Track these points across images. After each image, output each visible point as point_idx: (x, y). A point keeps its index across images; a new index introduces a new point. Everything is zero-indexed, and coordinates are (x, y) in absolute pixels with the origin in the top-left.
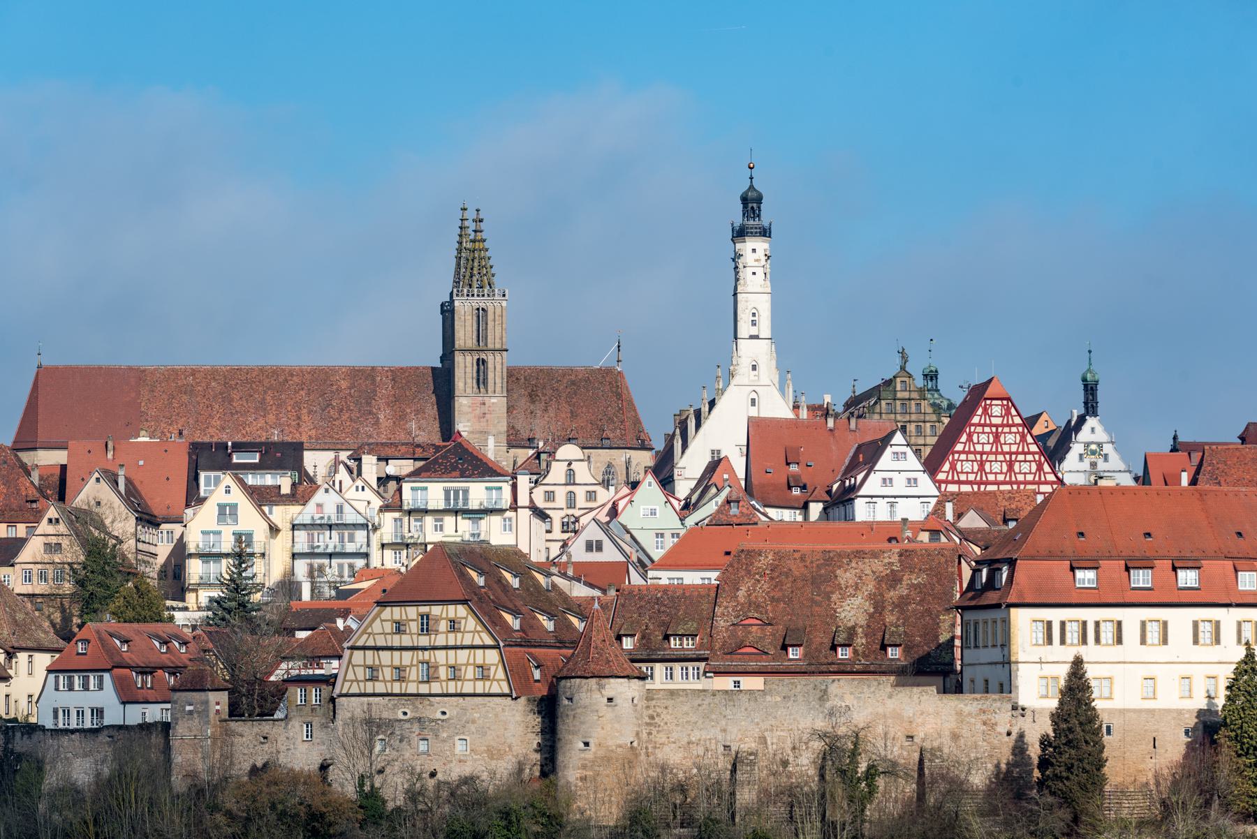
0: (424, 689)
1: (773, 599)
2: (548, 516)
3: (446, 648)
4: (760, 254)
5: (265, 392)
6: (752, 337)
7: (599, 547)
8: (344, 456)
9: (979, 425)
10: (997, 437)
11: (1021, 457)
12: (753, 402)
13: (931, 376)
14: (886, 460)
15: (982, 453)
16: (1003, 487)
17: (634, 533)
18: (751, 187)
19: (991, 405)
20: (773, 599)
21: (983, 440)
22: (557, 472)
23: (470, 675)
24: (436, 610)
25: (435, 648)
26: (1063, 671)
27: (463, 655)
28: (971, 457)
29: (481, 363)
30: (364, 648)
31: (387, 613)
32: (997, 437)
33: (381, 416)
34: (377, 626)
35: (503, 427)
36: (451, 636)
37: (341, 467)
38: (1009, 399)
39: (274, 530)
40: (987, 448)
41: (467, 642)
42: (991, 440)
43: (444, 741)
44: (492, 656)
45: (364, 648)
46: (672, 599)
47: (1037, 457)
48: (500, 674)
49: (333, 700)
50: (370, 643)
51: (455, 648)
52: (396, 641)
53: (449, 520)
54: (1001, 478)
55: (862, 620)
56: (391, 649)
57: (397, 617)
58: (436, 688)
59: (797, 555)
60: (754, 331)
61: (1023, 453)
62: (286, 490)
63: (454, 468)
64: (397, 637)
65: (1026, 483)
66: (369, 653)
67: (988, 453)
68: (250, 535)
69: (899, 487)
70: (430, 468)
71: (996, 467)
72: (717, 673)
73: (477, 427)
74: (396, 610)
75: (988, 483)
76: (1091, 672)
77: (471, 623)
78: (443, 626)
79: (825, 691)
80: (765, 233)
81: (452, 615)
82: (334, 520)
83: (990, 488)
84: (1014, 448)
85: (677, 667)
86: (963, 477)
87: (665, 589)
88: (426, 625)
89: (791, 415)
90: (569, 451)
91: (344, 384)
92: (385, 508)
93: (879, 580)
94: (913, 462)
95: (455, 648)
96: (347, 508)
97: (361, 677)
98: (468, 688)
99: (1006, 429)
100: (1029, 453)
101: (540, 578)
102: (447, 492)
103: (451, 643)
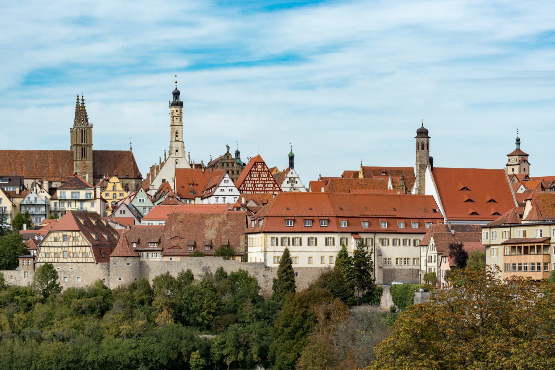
0: (65, 260)
1: (184, 230)
2: (107, 202)
3: (73, 247)
6: (176, 141)
7: (124, 213)
8: (37, 181)
10: (260, 175)
11: (268, 182)
12: (177, 163)
13: (237, 153)
14: (222, 184)
15: (254, 181)
16: (261, 192)
17: (137, 208)
18: (176, 89)
20: (184, 230)
22: (110, 187)
23: (81, 255)
24: (69, 234)
25: (69, 247)
26: (281, 255)
27: (78, 249)
28: (251, 182)
29: (83, 150)
30: (45, 246)
31: (52, 235)
32: (260, 175)
33: (50, 167)
34: (49, 239)
35: (91, 171)
36: (74, 242)
37: (37, 185)
38: (264, 162)
39: (14, 206)
40: (256, 179)
41: (79, 244)
43: (72, 278)
44: (88, 250)
45: (45, 246)
46: (150, 231)
48: (91, 256)
49: (34, 264)
50: (47, 245)
51: (76, 247)
52: (55, 244)
53: (73, 204)
54: (261, 189)
55: (214, 237)
56: (54, 247)
57: (55, 236)
58: (69, 260)
59: (192, 215)
60: (177, 139)
61: (268, 181)
62: (18, 192)
63: (75, 185)
64: (55, 243)
65: (269, 191)
66: (46, 248)
67: (257, 181)
68: (5, 208)
69: (226, 192)
70: (66, 185)
71: (259, 185)
72: (165, 255)
73: (83, 171)
74: (55, 233)
75: (256, 191)
76: (292, 255)
77: (81, 238)
78: (71, 239)
79: (201, 262)
81: (74, 235)
82: (33, 203)
83: (257, 192)
84: (265, 179)
85: (151, 253)
86: (248, 189)
87: (147, 227)
88: (65, 238)
89: (190, 167)
90: (114, 179)
91: (37, 156)
92: (51, 199)
93: (219, 223)
94: (231, 183)
95: (76, 247)
96: (38, 199)
97: (44, 256)
98: (80, 260)
101: (105, 223)
102: (72, 193)
103: (74, 245)
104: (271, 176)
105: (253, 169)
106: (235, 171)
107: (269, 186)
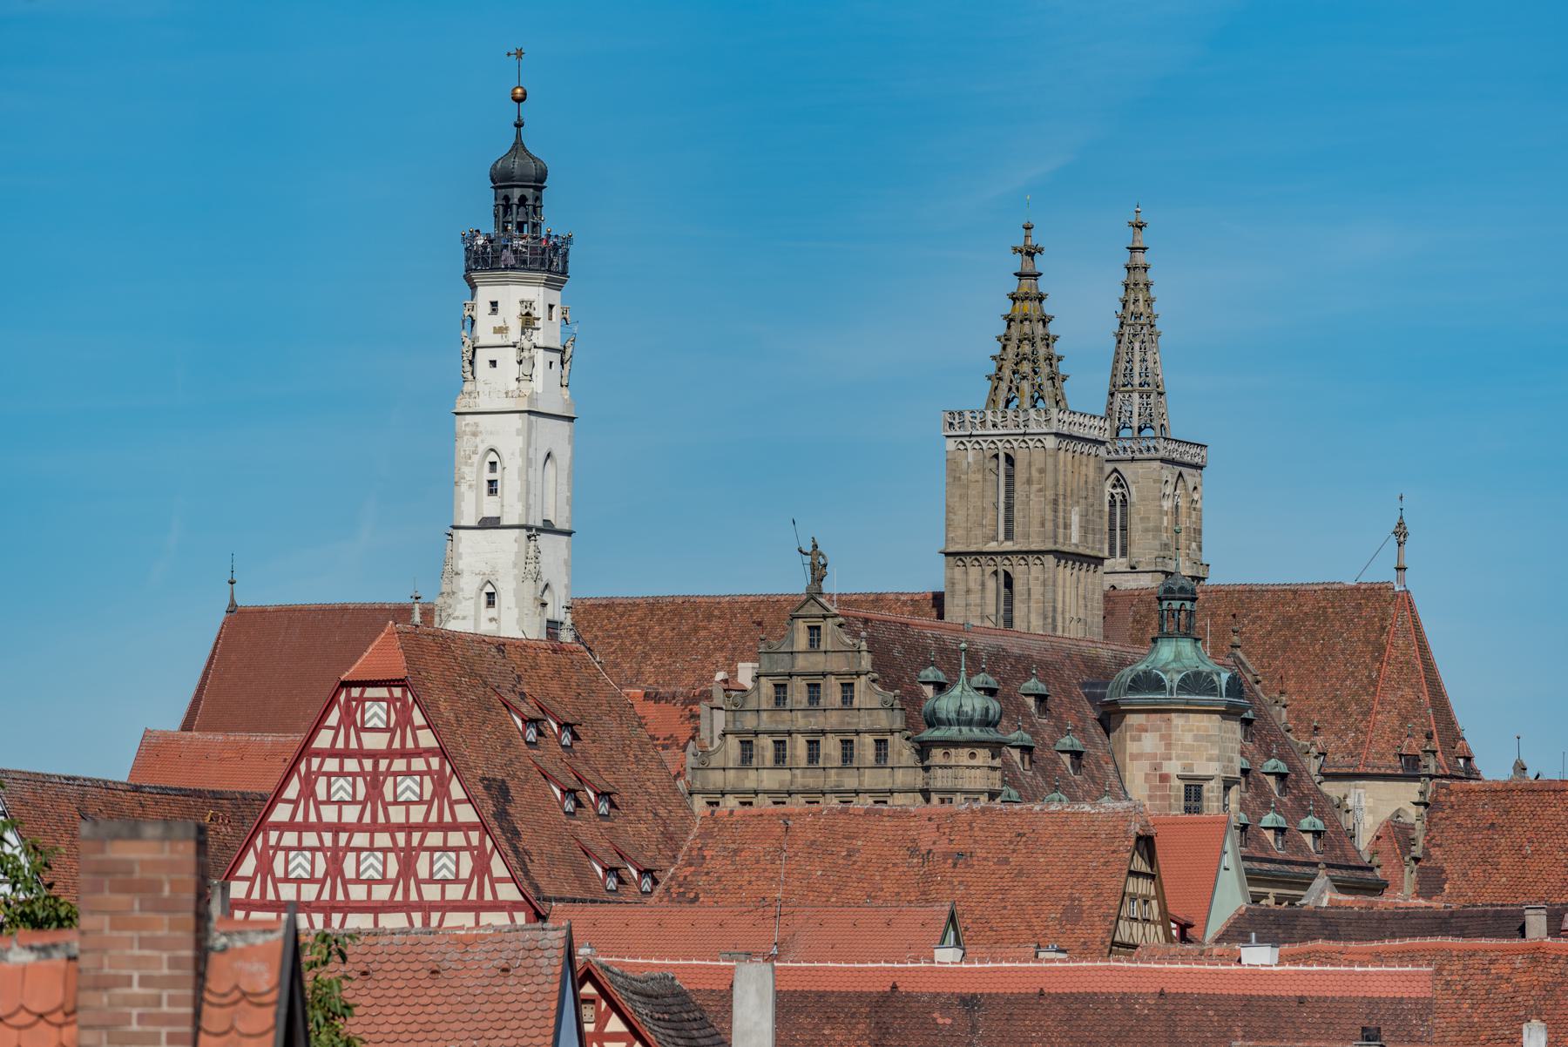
4: (511, 314)
5: (646, 656)
9: (332, 753)
10: (375, 786)
11: (434, 839)
15: (337, 828)
18: (518, 146)
19: (362, 700)
21: (340, 793)
28: (310, 839)
32: (375, 786)
40: (351, 814)
42: (361, 796)
47: (475, 837)
54: (382, 893)
60: (490, 508)
61: (441, 827)
65: (445, 907)
67: (351, 829)
75: (349, 908)
80: (549, 261)
99: (399, 764)
100: (456, 826)
104: (456, 791)
105: (323, 740)
106: (866, 747)
107: (445, 865)
